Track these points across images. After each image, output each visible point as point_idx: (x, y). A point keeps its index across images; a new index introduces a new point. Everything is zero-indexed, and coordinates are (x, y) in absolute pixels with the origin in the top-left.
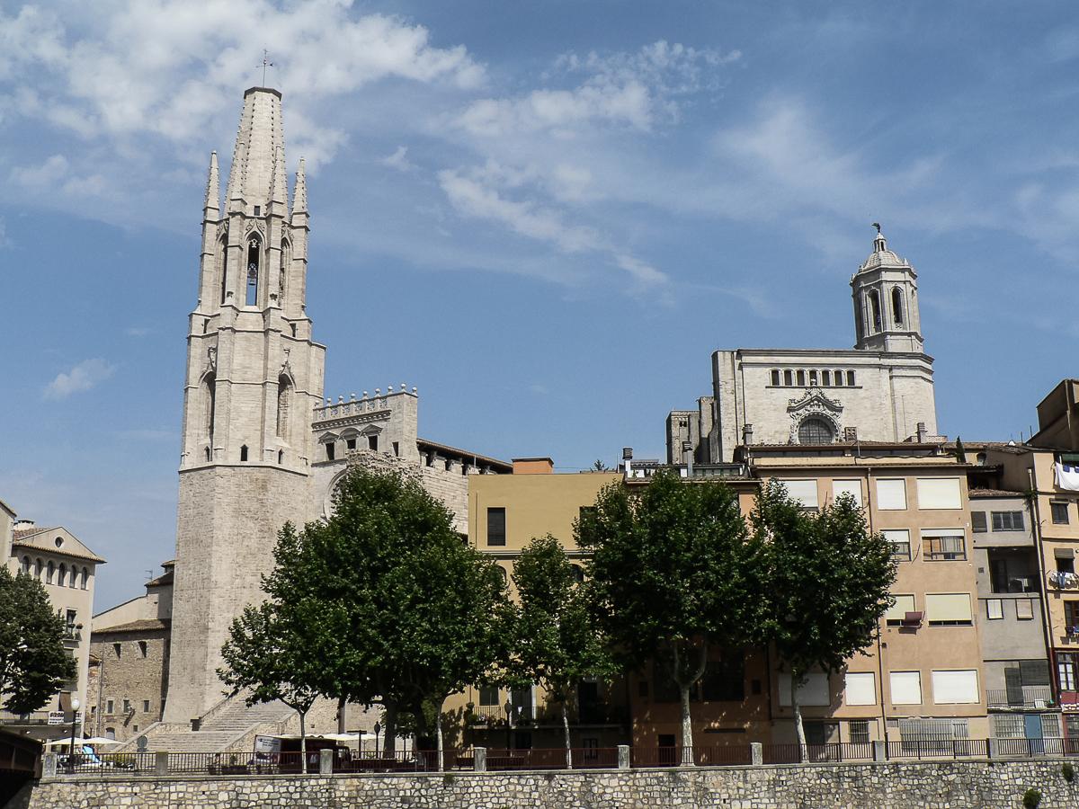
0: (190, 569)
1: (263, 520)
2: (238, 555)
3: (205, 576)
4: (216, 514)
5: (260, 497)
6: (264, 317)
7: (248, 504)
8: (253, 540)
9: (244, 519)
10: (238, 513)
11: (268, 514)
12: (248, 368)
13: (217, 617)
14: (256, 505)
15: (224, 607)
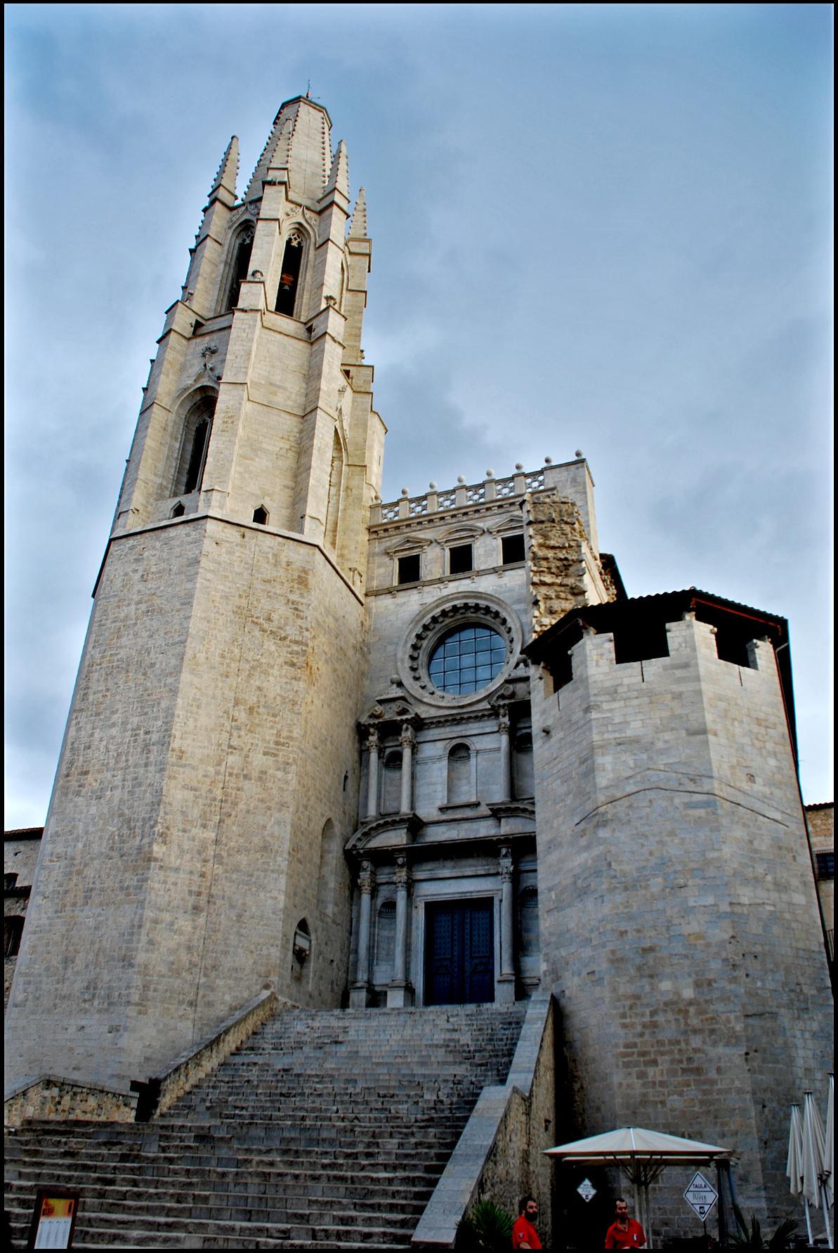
0: (114, 725)
1: (296, 642)
2: (237, 703)
3: (155, 737)
4: (197, 611)
5: (292, 597)
6: (310, 330)
7: (265, 604)
8: (271, 679)
9: (257, 633)
10: (246, 617)
11: (306, 634)
12: (279, 387)
13: (175, 834)
14: (281, 611)
15: (196, 813)
